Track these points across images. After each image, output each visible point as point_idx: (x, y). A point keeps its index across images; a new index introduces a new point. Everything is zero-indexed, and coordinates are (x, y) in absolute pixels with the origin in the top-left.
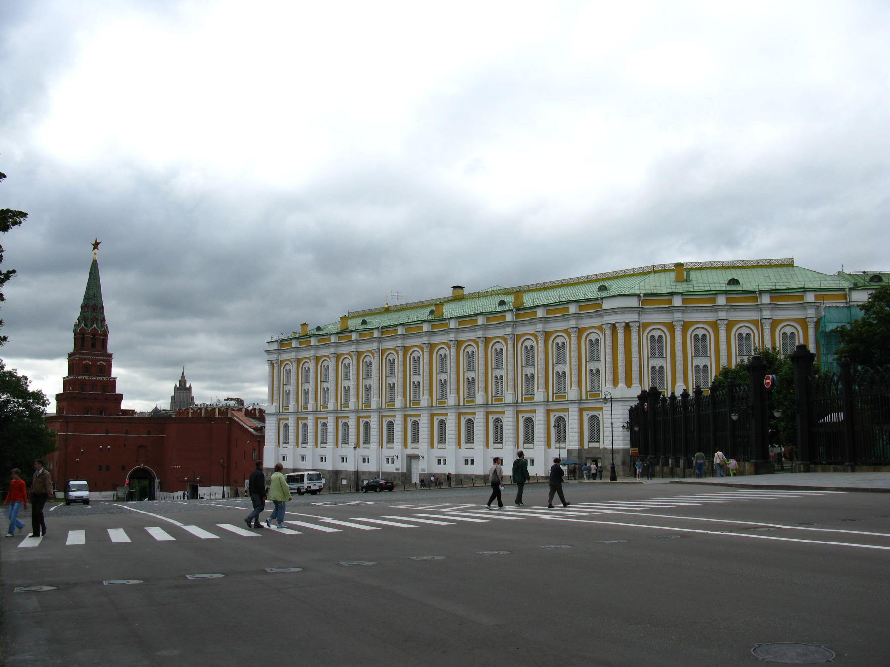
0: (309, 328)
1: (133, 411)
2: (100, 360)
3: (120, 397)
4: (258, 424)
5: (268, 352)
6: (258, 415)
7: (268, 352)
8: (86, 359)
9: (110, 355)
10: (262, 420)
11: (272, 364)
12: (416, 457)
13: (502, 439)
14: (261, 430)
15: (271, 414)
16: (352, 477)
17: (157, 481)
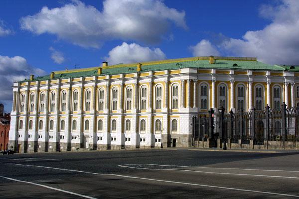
4: (5, 121)
10: (10, 119)
12: (88, 136)
13: (130, 129)
16: (55, 145)
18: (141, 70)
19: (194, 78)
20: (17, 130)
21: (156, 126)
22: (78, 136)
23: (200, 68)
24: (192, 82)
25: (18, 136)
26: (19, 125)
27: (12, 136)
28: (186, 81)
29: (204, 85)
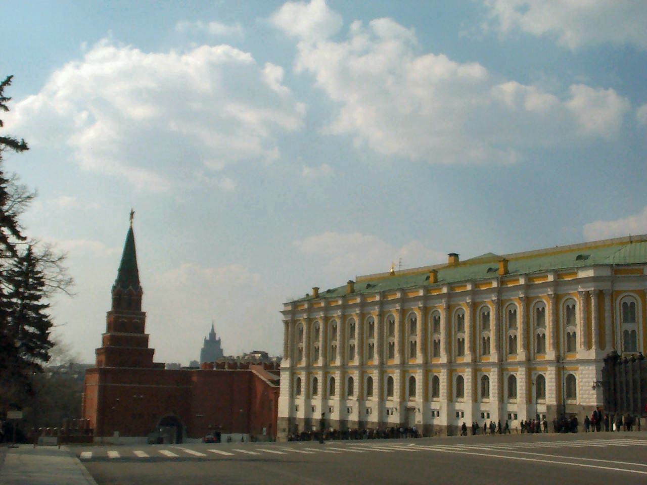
0: (320, 291)
1: (163, 364)
2: (134, 318)
3: (152, 352)
4: (275, 378)
5: (284, 313)
6: (273, 367)
7: (284, 313)
8: (123, 317)
9: (144, 314)
10: (278, 374)
11: (286, 323)
14: (278, 382)
15: (285, 369)
17: (185, 428)
18: (506, 272)
19: (606, 286)
20: (292, 397)
21: (537, 386)
22: (396, 409)
23: (617, 265)
24: (600, 294)
25: (294, 408)
26: (295, 390)
27: (283, 410)
28: (587, 295)
29: (628, 301)
